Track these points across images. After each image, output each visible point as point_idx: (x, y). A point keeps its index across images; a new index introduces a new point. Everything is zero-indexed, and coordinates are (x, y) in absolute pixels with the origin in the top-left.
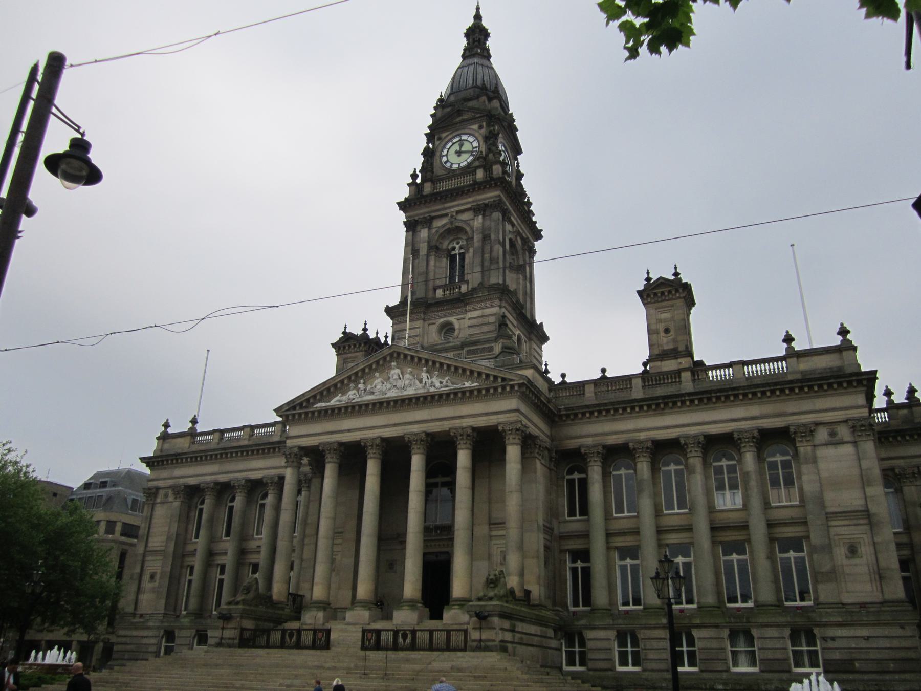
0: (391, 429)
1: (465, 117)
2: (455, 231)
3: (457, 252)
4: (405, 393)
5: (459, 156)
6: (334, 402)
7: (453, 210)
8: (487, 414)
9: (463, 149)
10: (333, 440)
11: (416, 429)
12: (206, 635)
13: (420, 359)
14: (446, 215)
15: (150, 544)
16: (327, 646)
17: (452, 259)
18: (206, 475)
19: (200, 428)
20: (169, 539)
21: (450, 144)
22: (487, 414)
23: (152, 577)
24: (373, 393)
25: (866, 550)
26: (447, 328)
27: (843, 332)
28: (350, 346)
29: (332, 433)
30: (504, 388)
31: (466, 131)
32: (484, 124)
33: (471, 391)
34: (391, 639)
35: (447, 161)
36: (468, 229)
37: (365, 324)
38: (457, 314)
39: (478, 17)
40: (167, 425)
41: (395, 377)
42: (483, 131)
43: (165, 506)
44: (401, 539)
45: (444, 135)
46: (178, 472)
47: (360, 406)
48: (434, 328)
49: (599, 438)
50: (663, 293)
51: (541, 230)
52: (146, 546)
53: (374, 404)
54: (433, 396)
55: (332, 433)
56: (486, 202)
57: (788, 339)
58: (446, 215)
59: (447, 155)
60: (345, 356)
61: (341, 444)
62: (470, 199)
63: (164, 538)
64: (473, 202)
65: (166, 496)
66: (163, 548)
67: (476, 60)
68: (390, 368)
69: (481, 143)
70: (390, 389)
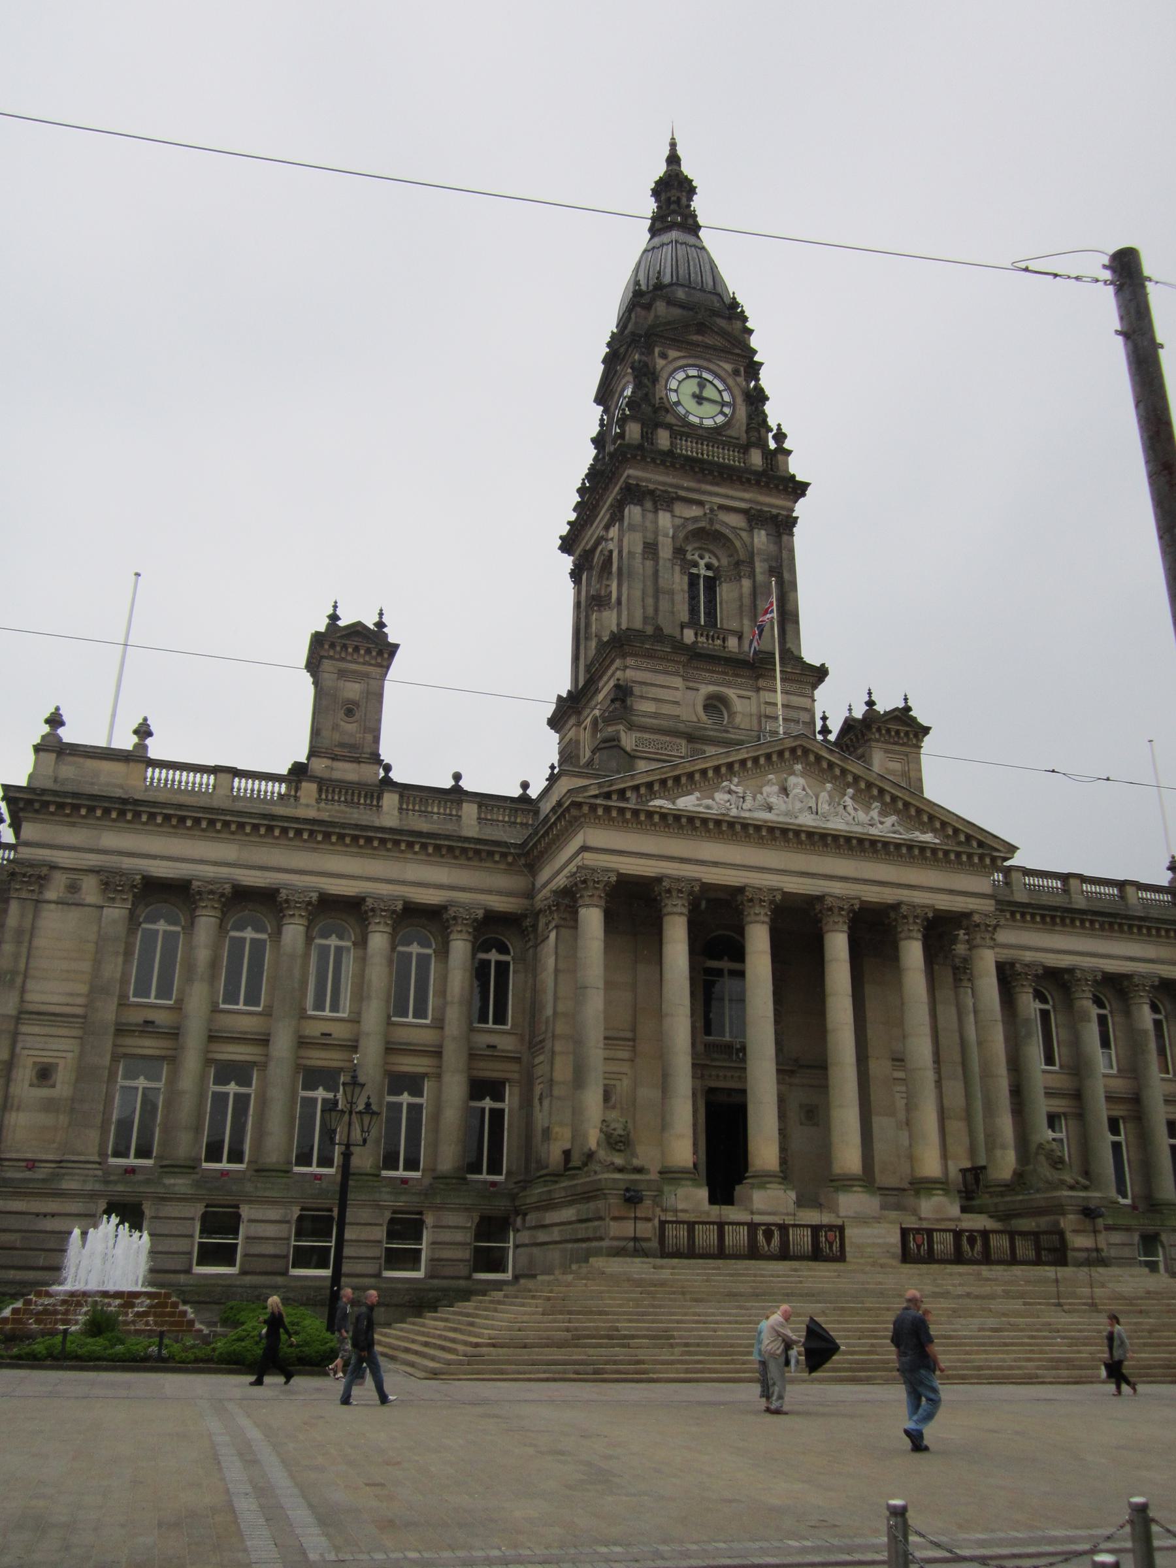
0: (795, 879)
1: (709, 340)
2: (706, 536)
3: (703, 572)
4: (830, 825)
5: (700, 403)
6: (688, 803)
8: (951, 892)
9: (706, 394)
10: (682, 873)
11: (837, 888)
12: (238, 1217)
13: (844, 771)
14: (700, 503)
15: (29, 997)
16: (841, 1257)
17: (693, 580)
18: (202, 862)
19: (155, 749)
20: (97, 990)
21: (721, 387)
22: (951, 892)
23: (44, 1074)
24: (770, 809)
26: (716, 704)
28: (356, 649)
29: (683, 860)
30: (982, 857)
31: (711, 366)
32: (742, 369)
33: (934, 851)
34: (950, 1248)
35: (678, 403)
36: (738, 544)
37: (335, 607)
38: (740, 686)
39: (673, 159)
40: (55, 721)
41: (798, 790)
42: (740, 380)
43: (74, 914)
44: (788, 1068)
45: (673, 354)
46: (112, 839)
47: (745, 826)
48: (700, 697)
49: (1012, 952)
50: (898, 732)
51: (561, 537)
52: (22, 1001)
53: (771, 830)
54: (873, 842)
55: (683, 860)
56: (775, 511)
59: (676, 391)
60: (343, 665)
61: (706, 887)
62: (747, 496)
63: (83, 989)
64: (750, 501)
65: (73, 888)
66: (79, 1011)
67: (674, 234)
68: (793, 773)
69: (739, 400)
70: (801, 811)
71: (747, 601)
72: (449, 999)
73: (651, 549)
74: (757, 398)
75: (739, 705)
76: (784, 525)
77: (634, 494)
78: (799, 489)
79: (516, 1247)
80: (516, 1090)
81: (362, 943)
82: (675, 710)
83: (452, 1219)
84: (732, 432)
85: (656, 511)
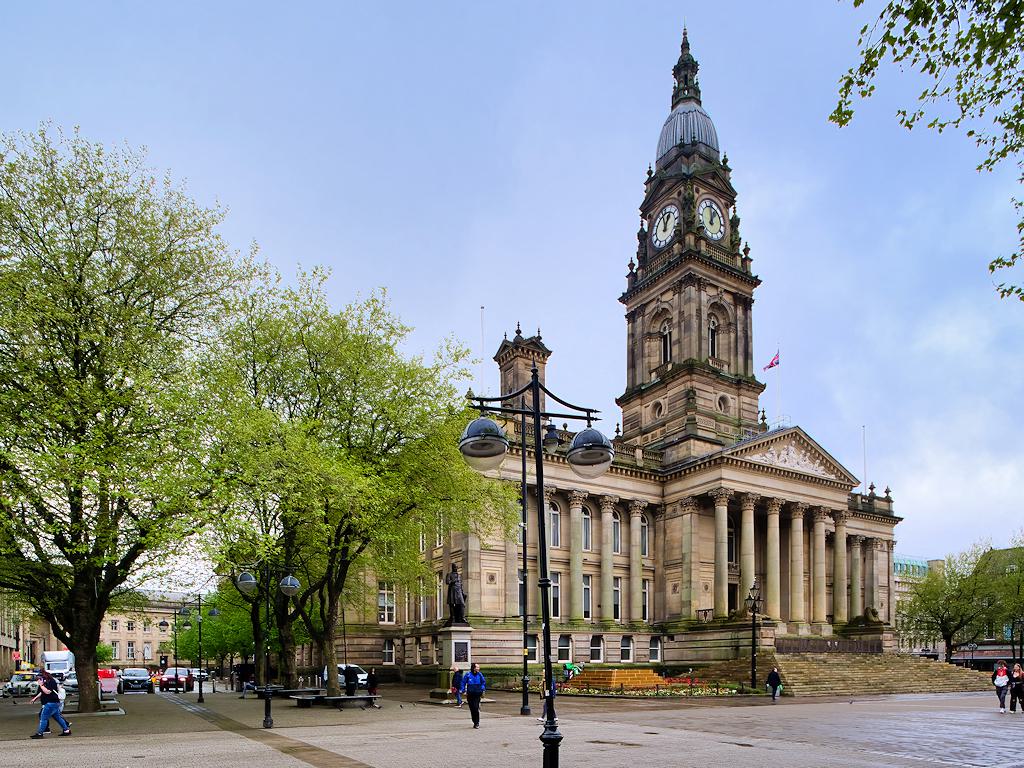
7: (724, 287)
14: (717, 287)
25: (886, 605)
26: (723, 400)
27: (887, 491)
57: (872, 488)
58: (717, 287)
64: (736, 288)
69: (728, 223)
71: (732, 345)
72: (633, 543)
73: (699, 311)
74: (735, 223)
75: (731, 403)
76: (746, 303)
77: (691, 279)
78: (756, 282)
79: (663, 649)
80: (651, 584)
81: (599, 517)
82: (709, 404)
83: (642, 638)
84: (724, 244)
85: (699, 290)
